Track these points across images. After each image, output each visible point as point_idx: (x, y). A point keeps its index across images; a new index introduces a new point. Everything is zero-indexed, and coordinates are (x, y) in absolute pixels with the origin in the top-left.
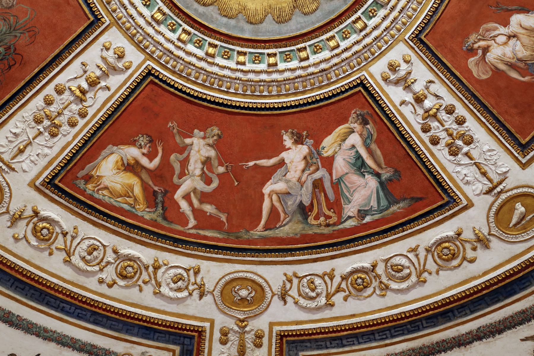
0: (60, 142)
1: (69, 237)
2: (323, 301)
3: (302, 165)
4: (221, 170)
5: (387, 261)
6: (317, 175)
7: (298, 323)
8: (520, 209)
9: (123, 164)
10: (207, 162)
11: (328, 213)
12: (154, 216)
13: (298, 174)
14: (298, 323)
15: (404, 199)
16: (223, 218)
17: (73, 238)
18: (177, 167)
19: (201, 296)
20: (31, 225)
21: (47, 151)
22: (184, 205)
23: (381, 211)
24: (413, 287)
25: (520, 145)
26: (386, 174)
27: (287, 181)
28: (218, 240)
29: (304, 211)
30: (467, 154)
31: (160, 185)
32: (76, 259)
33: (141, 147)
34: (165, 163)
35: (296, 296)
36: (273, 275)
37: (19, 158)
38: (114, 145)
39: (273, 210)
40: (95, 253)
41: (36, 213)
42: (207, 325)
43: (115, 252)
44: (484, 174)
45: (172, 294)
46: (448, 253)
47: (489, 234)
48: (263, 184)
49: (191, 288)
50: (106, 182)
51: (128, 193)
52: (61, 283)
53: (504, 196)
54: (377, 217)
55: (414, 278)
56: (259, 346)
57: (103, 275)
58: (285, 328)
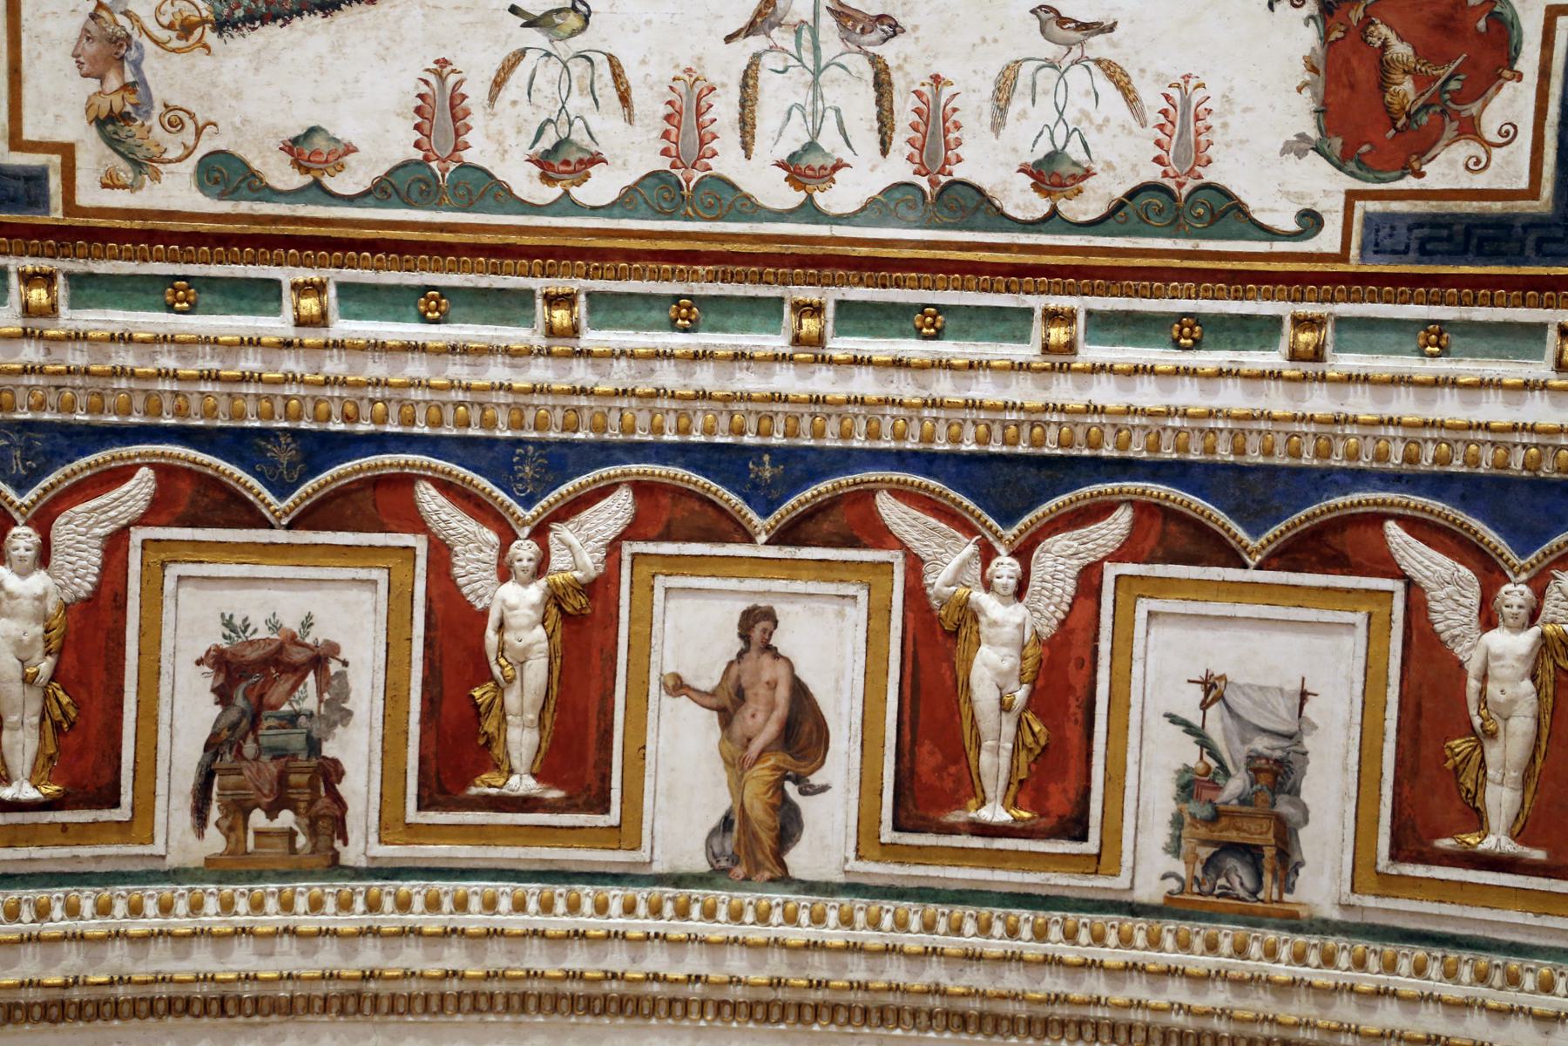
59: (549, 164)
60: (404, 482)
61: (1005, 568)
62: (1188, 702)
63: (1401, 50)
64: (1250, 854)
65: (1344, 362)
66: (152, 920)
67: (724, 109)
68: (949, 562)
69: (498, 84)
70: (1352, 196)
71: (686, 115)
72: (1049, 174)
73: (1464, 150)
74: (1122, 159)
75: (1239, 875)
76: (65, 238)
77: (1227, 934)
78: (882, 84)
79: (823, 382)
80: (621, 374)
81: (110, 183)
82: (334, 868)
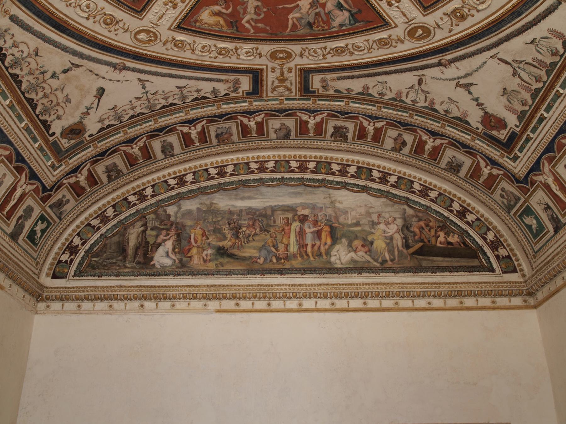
0: (178, 10)
1: (192, 45)
2: (321, 57)
3: (309, 6)
4: (265, 10)
5: (353, 44)
6: (317, 10)
7: (309, 64)
8: (420, 32)
9: (213, 13)
10: (257, 7)
11: (323, 25)
12: (232, 31)
13: (306, 10)
14: (309, 64)
15: (363, 21)
16: (268, 28)
17: (194, 45)
18: (241, 11)
19: (260, 57)
20: (173, 44)
21: (174, 15)
22: (247, 25)
23: (351, 25)
24: (366, 54)
25: (424, 6)
26: (354, 11)
27: (301, 13)
28: (266, 37)
29: (310, 25)
30: (397, 7)
31: (234, 21)
32: (197, 52)
33: (221, 5)
34: (235, 11)
35: (308, 55)
36: (296, 48)
37: (161, 21)
38: (206, 6)
39: (294, 25)
40: (206, 48)
41: (174, 39)
42: (264, 67)
43: (215, 46)
44: (405, 15)
45: (245, 58)
46: (383, 43)
47: (404, 38)
48: (288, 14)
49: (255, 55)
50: (205, 21)
51: (218, 23)
52: (192, 61)
53: (413, 26)
54: (348, 27)
55: (366, 51)
56: (291, 72)
57: (211, 55)
58: (302, 66)
59: (379, 94)
60: (358, 117)
61: (432, 140)
62: (451, 157)
63: (493, 120)
64: (455, 170)
65: (477, 142)
66: (326, 144)
67: (404, 94)
68: (425, 137)
69: (374, 87)
70: (483, 129)
71: (399, 93)
72: (446, 111)
73: (497, 132)
74: (456, 113)
75: (453, 171)
76: (318, 96)
77: (450, 173)
78: (426, 97)
79: (412, 120)
80: (386, 113)
81: (323, 91)
82: (346, 142)
